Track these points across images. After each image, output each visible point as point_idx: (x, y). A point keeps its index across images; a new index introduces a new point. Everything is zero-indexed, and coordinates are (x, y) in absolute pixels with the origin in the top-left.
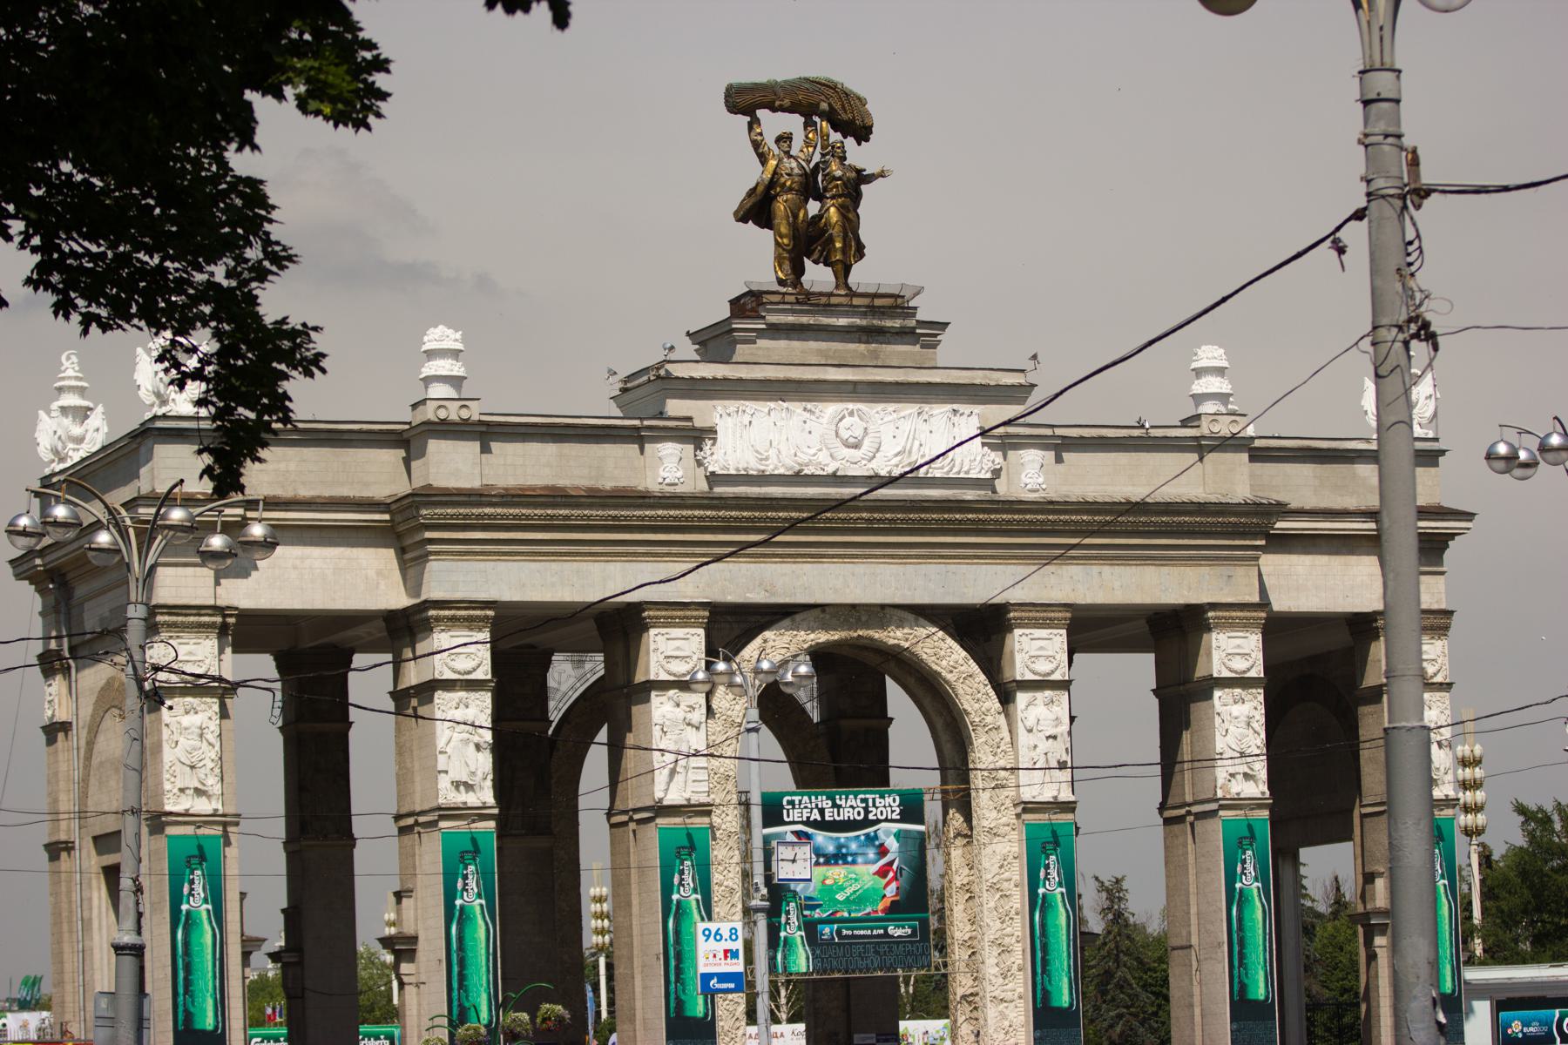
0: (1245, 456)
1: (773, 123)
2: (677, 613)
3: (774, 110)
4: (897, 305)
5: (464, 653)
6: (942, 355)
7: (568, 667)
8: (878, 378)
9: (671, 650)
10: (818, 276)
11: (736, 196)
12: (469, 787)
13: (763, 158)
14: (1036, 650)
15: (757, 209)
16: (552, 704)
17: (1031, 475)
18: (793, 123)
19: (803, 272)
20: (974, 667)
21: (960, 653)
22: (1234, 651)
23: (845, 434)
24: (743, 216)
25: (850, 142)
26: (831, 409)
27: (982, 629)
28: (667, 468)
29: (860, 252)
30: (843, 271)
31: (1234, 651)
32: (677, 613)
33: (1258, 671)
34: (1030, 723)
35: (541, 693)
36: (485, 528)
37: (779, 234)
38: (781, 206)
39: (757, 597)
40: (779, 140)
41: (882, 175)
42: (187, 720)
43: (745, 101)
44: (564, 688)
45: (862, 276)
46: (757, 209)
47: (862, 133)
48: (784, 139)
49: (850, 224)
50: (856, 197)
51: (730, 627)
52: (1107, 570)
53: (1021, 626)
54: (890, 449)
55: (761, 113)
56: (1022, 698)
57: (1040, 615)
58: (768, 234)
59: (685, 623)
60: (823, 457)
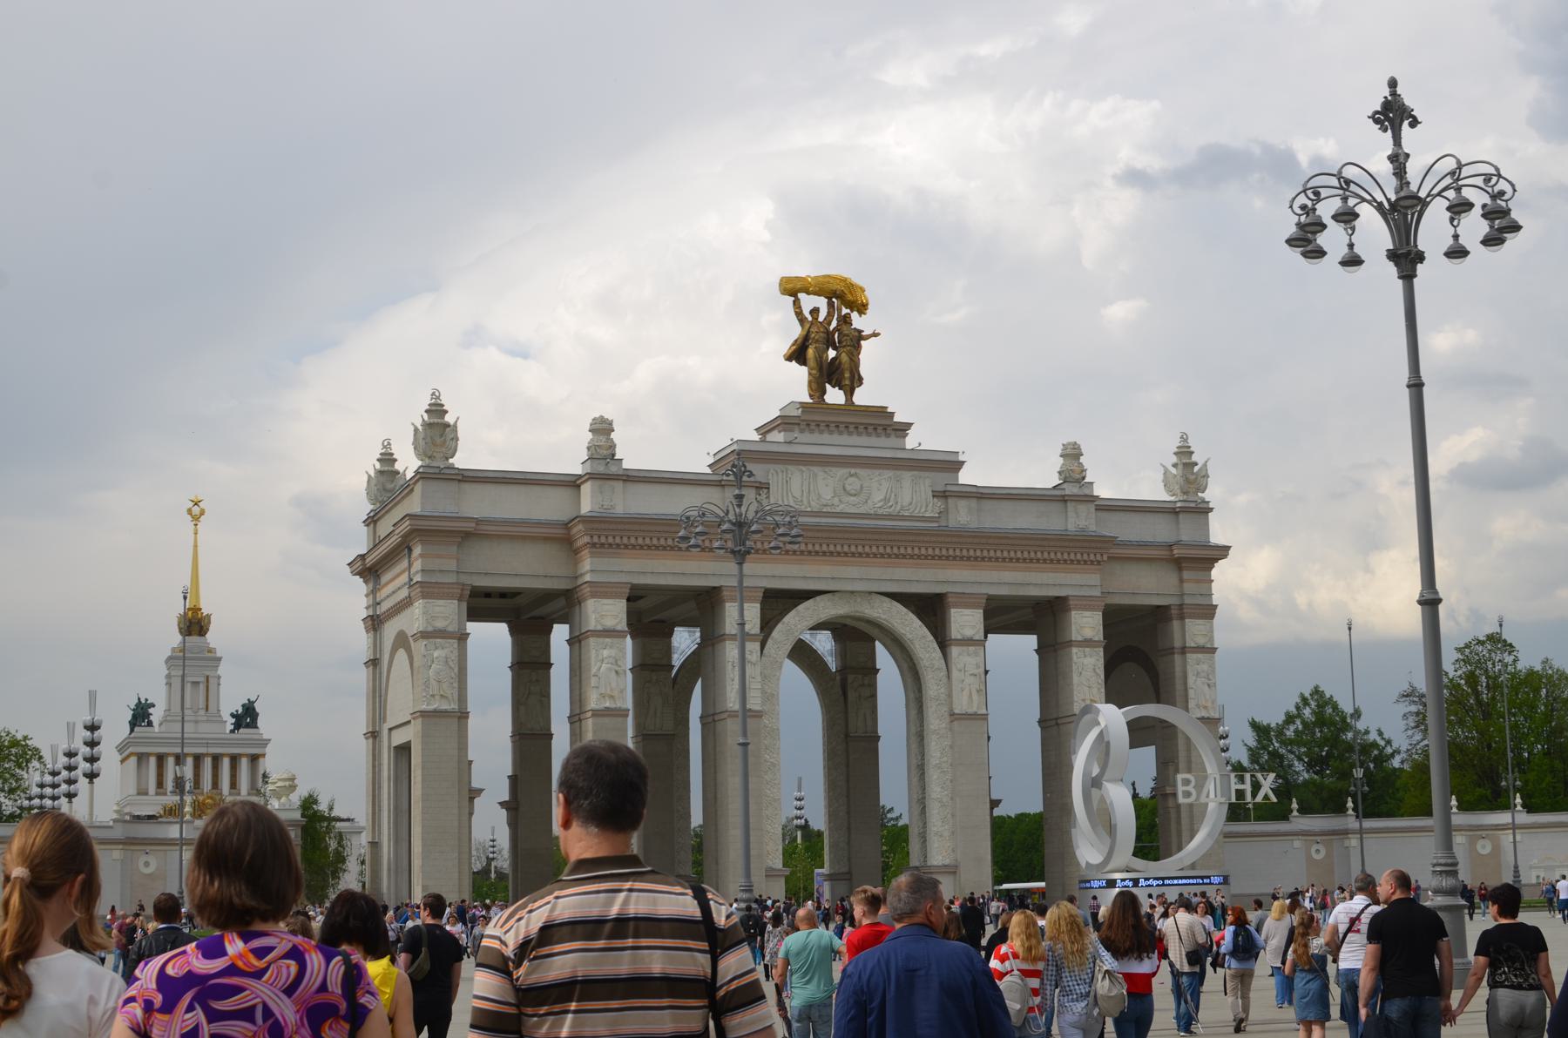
0: (1092, 507)
3: (808, 293)
4: (882, 413)
5: (607, 613)
6: (910, 442)
7: (686, 635)
8: (864, 440)
10: (834, 396)
11: (786, 346)
12: (612, 697)
13: (802, 320)
14: (965, 621)
15: (798, 354)
16: (675, 656)
17: (963, 516)
18: (821, 303)
19: (824, 392)
23: (848, 488)
24: (789, 358)
25: (855, 315)
26: (841, 472)
29: (860, 381)
30: (850, 393)
31: (1086, 624)
33: (1100, 637)
34: (960, 666)
35: (668, 651)
37: (810, 369)
38: (811, 352)
40: (811, 312)
41: (875, 335)
42: (436, 654)
43: (792, 288)
44: (683, 647)
45: (861, 397)
46: (798, 354)
47: (862, 308)
48: (815, 311)
49: (855, 365)
50: (858, 347)
53: (956, 606)
54: (877, 497)
55: (801, 296)
56: (955, 651)
57: (966, 601)
58: (804, 369)
60: (836, 501)
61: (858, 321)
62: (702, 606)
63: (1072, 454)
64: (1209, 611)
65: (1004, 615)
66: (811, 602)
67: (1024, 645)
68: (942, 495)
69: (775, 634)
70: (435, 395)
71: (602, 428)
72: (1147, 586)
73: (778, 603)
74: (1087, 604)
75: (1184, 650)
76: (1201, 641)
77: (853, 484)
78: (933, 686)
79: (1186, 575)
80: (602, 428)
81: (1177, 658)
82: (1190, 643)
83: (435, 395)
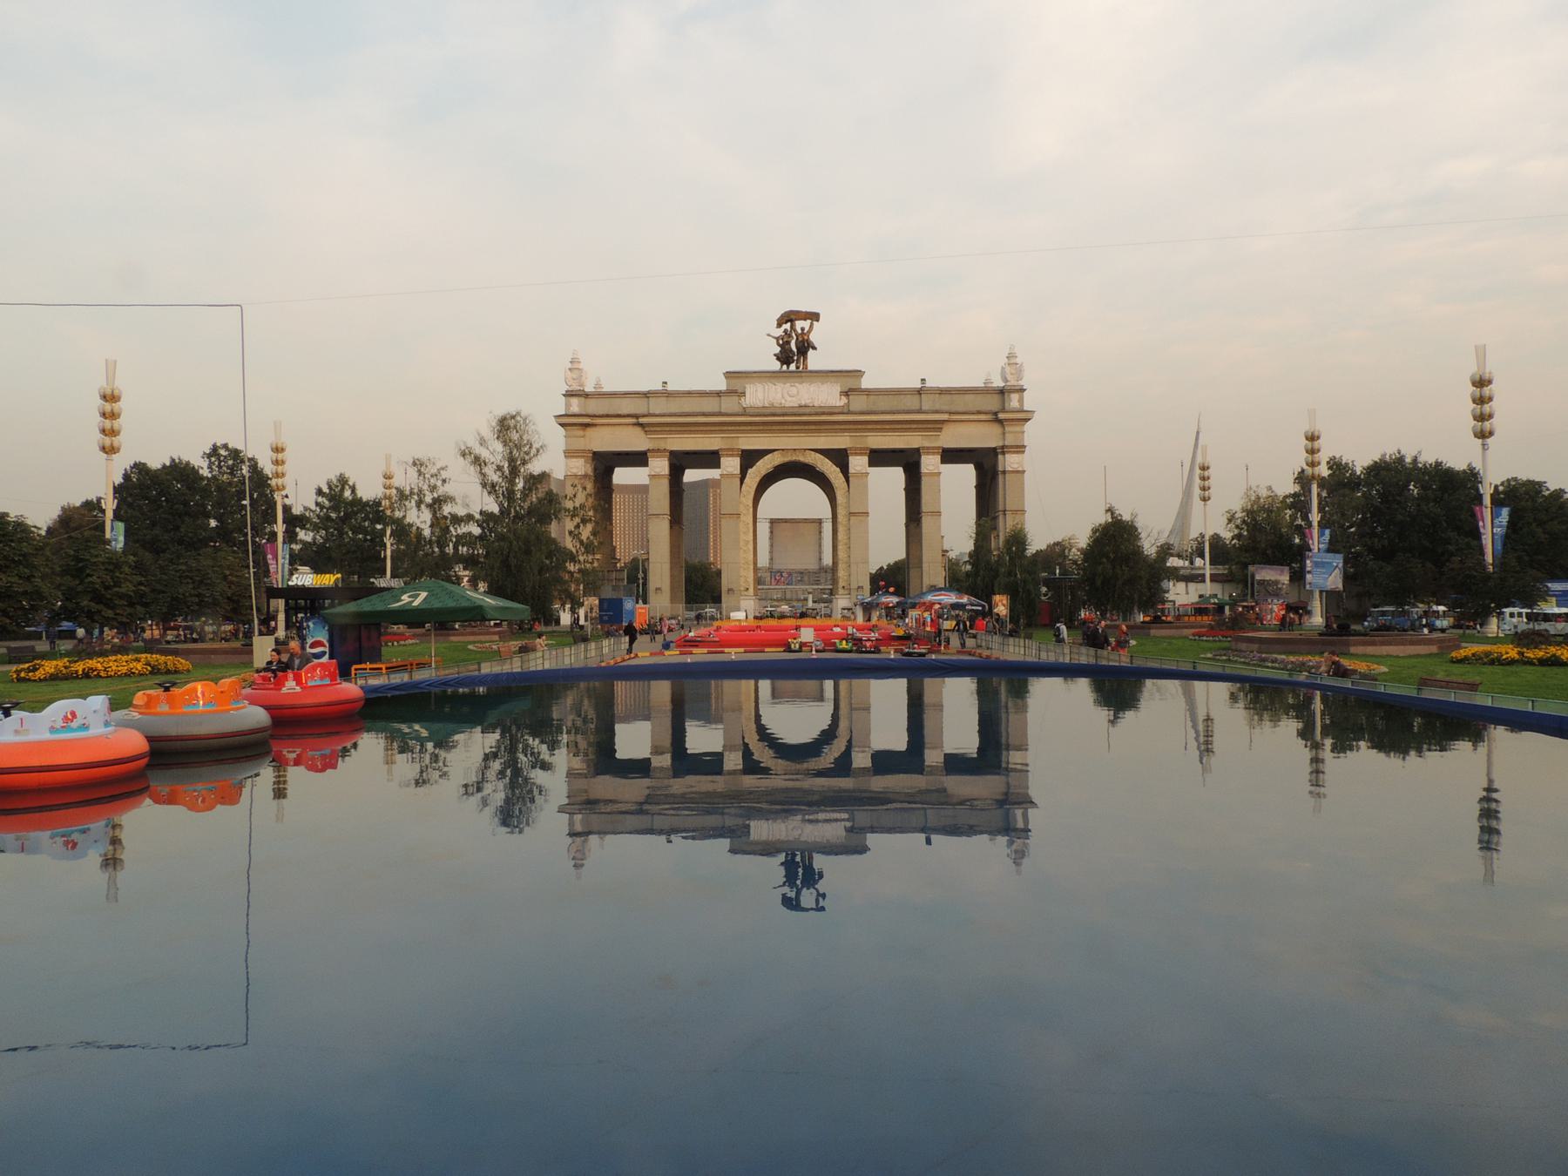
2: (730, 452)
14: (858, 463)
17: (858, 403)
22: (929, 463)
27: (840, 458)
28: (728, 404)
57: (859, 452)
62: (710, 459)
64: (1020, 449)
65: (879, 458)
67: (897, 475)
68: (846, 393)
72: (979, 436)
73: (749, 458)
75: (1004, 472)
76: (1016, 466)
77: (794, 391)
78: (840, 499)
81: (1000, 477)
82: (1008, 468)
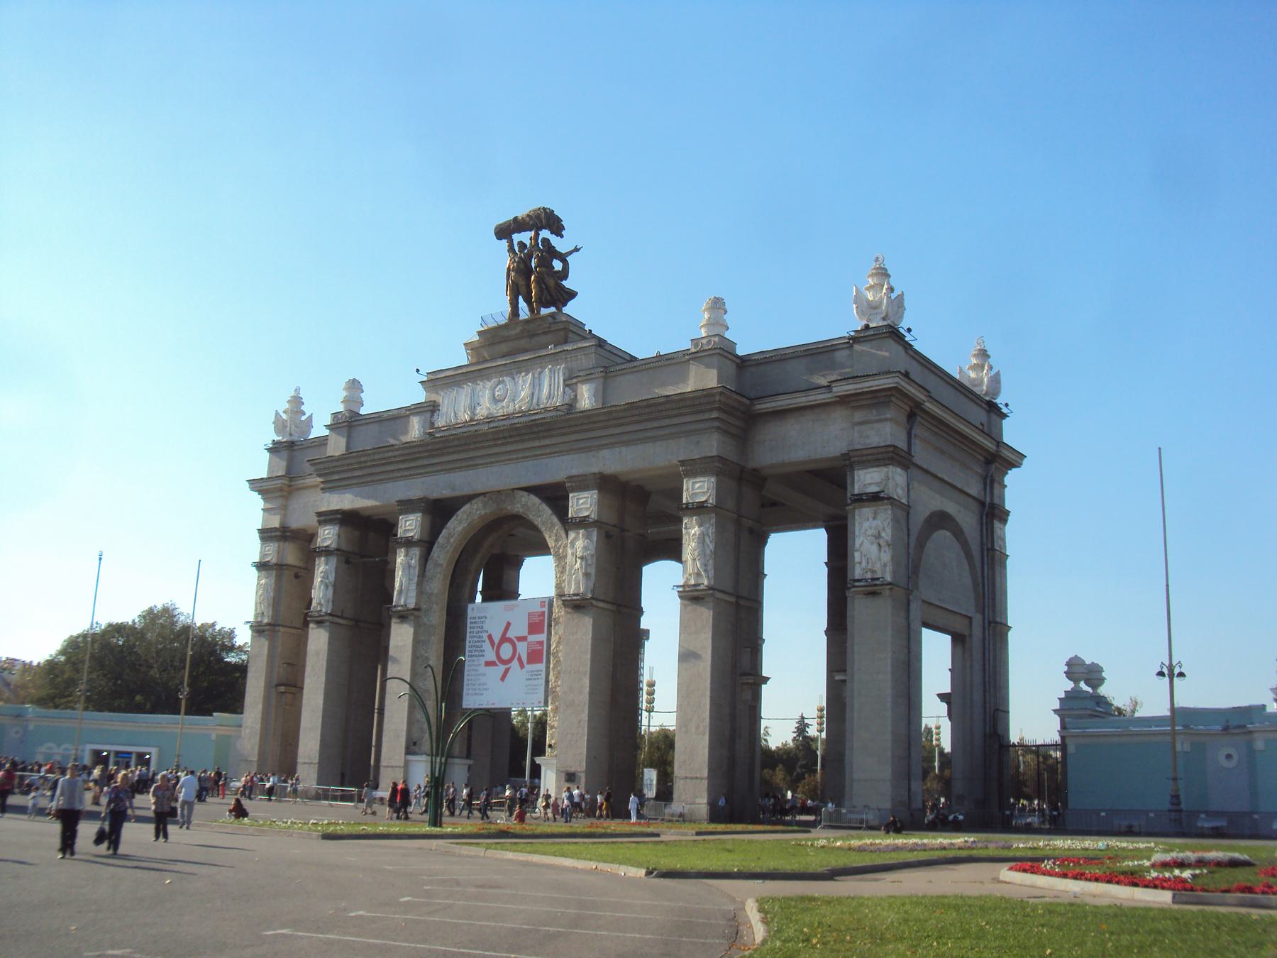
1: (517, 238)
9: (410, 525)
14: (583, 504)
17: (586, 397)
20: (555, 519)
21: (546, 510)
26: (489, 384)
32: (407, 506)
36: (338, 472)
39: (446, 493)
41: (577, 250)
51: (439, 512)
52: (624, 449)
53: (572, 491)
57: (582, 483)
59: (413, 511)
61: (554, 240)
63: (717, 305)
66: (466, 508)
69: (441, 540)
70: (297, 390)
71: (354, 386)
74: (694, 468)
79: (859, 416)
80: (354, 386)
83: (297, 390)
